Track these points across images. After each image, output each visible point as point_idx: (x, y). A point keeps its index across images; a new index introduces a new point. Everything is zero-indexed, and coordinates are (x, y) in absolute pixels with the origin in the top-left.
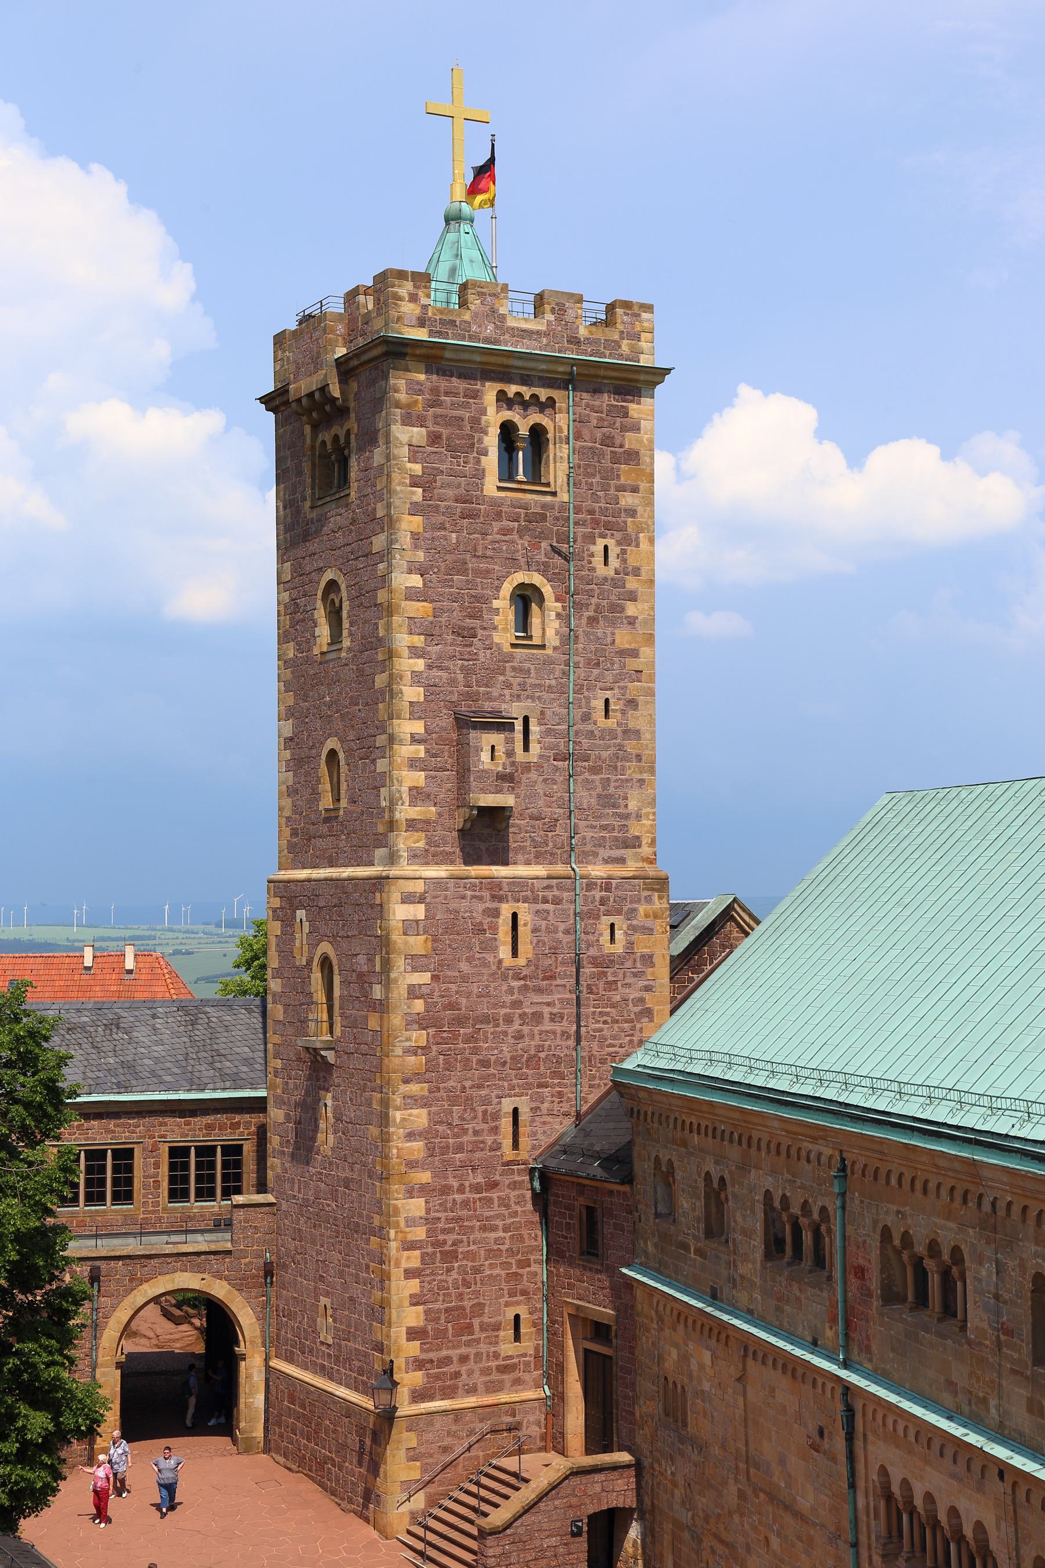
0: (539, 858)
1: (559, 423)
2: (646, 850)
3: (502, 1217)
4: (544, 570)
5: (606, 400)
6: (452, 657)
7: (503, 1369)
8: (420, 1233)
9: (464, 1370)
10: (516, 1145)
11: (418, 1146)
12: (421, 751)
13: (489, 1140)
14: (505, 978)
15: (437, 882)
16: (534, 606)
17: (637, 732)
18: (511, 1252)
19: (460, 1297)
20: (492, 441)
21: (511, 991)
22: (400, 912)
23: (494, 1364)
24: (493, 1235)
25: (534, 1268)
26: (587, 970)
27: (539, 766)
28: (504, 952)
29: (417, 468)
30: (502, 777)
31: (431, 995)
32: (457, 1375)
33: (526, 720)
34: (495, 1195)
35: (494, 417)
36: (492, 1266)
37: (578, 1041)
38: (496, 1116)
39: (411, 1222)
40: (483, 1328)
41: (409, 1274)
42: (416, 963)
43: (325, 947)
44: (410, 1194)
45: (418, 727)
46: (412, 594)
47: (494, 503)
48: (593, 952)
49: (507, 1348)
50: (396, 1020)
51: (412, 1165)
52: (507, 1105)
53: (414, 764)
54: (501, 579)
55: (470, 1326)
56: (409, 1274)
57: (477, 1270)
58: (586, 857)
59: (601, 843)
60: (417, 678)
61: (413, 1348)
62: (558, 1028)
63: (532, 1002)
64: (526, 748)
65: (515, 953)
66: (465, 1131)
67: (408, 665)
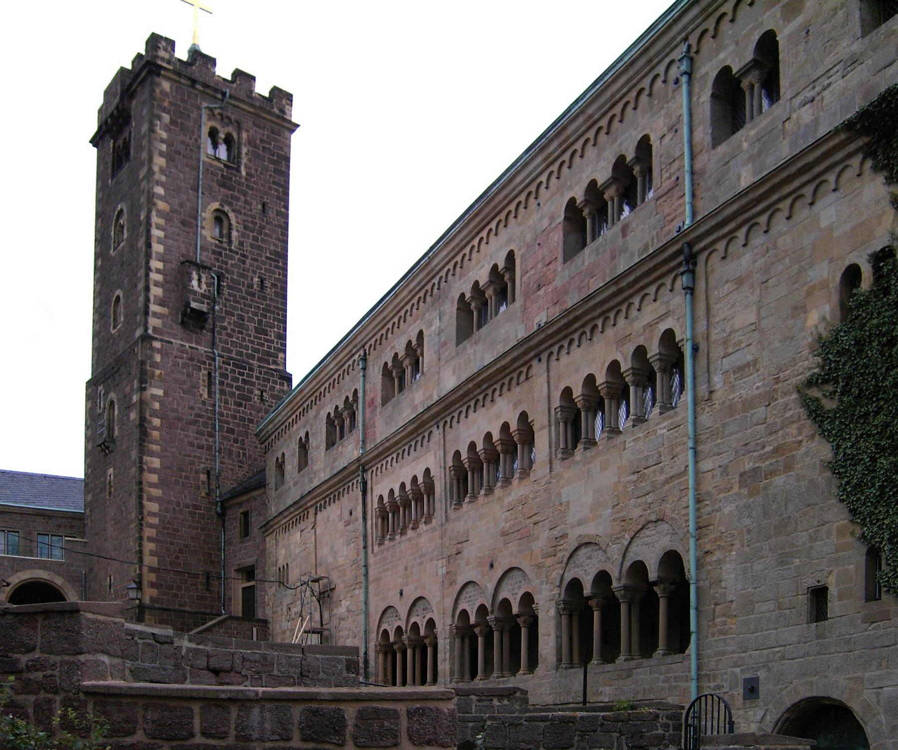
6: (178, 235)
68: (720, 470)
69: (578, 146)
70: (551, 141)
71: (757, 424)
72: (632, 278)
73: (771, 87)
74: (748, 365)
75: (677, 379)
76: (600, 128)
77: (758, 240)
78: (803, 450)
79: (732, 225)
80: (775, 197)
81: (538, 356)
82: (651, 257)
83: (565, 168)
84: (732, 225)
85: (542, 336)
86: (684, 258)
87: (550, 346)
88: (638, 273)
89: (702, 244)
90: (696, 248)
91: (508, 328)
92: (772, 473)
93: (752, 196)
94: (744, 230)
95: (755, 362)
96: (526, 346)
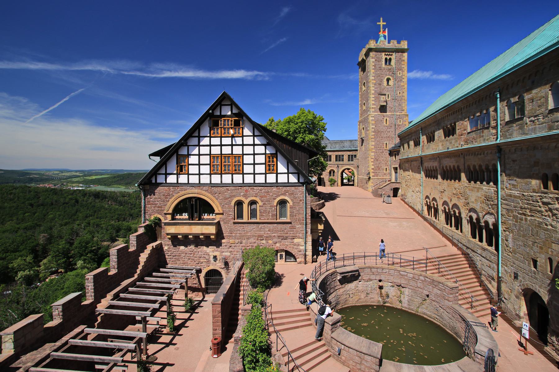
4: (391, 76)
5: (400, 54)
11: (373, 147)
20: (384, 60)
22: (371, 118)
28: (385, 123)
35: (384, 57)
42: (373, 124)
46: (373, 80)
50: (370, 131)
53: (373, 101)
58: (396, 112)
60: (373, 90)
67: (372, 88)
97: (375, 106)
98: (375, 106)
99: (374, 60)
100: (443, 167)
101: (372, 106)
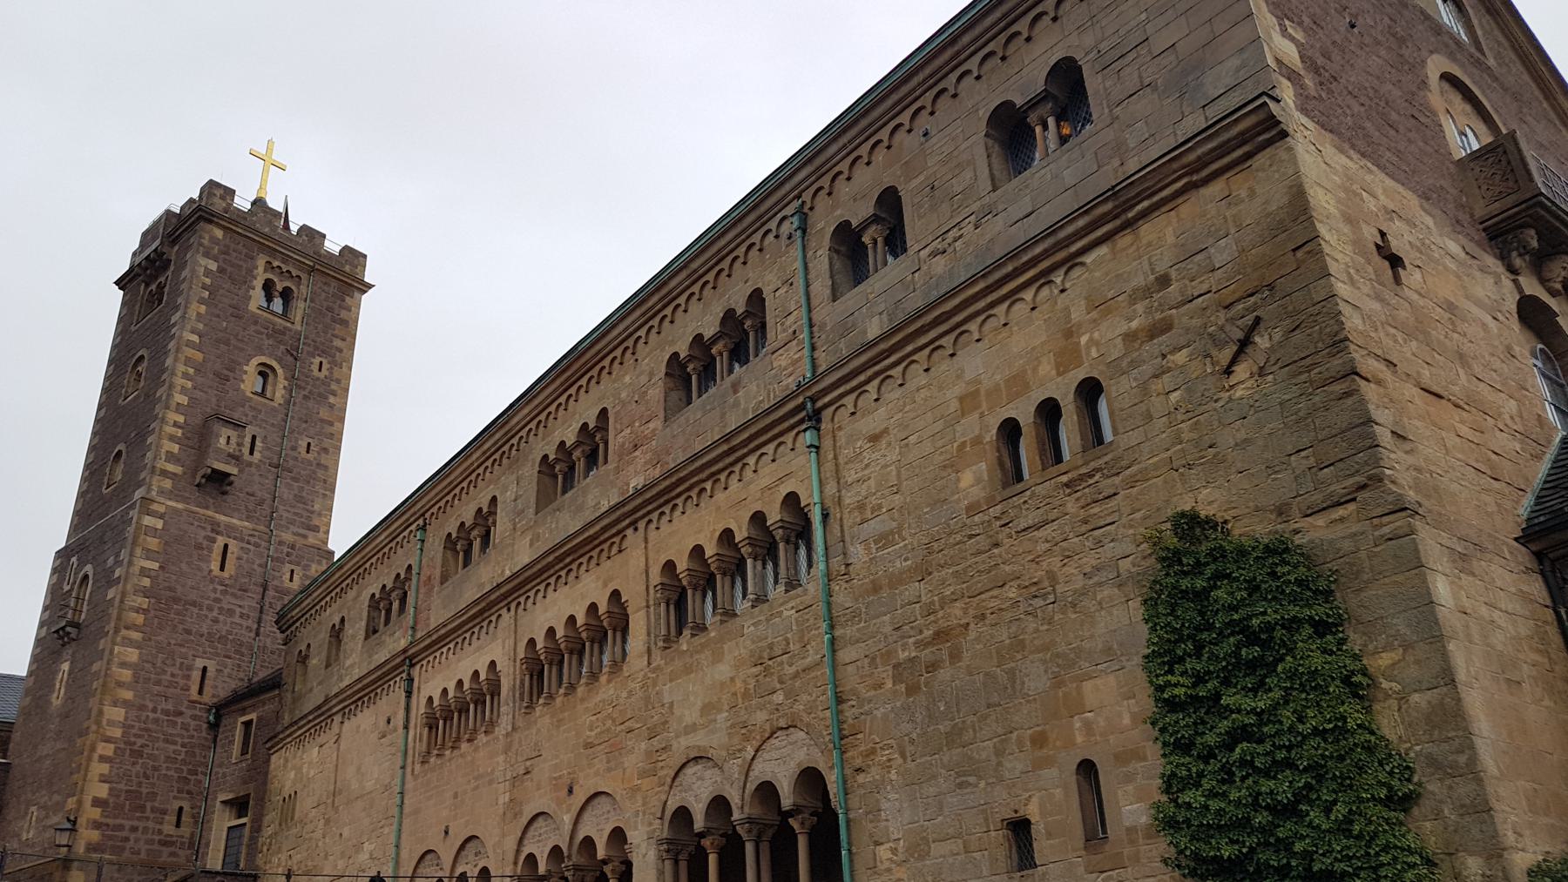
0: (248, 518)
1: (302, 290)
2: (321, 535)
3: (182, 736)
4: (279, 361)
7: (164, 843)
8: (117, 733)
9: (132, 836)
10: (200, 692)
11: (127, 675)
12: (180, 433)
13: (182, 682)
14: (212, 581)
15: (175, 510)
16: (271, 377)
17: (326, 468)
18: (184, 762)
19: (140, 784)
20: (258, 283)
21: (215, 590)
23: (157, 838)
24: (173, 747)
25: (200, 777)
26: (271, 593)
27: (258, 466)
28: (215, 566)
29: (208, 281)
30: (230, 455)
31: (156, 577)
32: (127, 839)
33: (254, 438)
34: (179, 720)
36: (168, 769)
37: (257, 634)
38: (190, 668)
39: (111, 723)
40: (153, 810)
41: (103, 759)
43: (89, 568)
44: (115, 704)
45: (181, 419)
46: (189, 344)
47: (254, 315)
48: (276, 583)
49: (168, 828)
51: (120, 684)
52: (199, 663)
53: (172, 438)
54: (251, 357)
55: (142, 808)
56: (103, 759)
57: (155, 769)
59: (292, 522)
61: (96, 813)
62: (245, 623)
63: (227, 603)
64: (251, 453)
65: (222, 569)
66: (164, 672)
67: (179, 381)
68: (867, 661)
69: (682, 300)
70: (652, 294)
71: (910, 603)
72: (745, 435)
73: (896, 243)
74: (892, 532)
75: (802, 552)
76: (707, 282)
77: (892, 394)
78: (972, 635)
79: (862, 378)
80: (909, 348)
81: (634, 524)
82: (768, 412)
83: (666, 323)
84: (862, 378)
85: (639, 501)
86: (806, 411)
87: (649, 513)
88: (753, 430)
89: (827, 399)
90: (819, 404)
91: (597, 495)
92: (933, 667)
93: (883, 346)
94: (876, 382)
95: (900, 528)
96: (618, 513)
97: (178, 470)
98: (178, 470)
99: (213, 266)
100: (532, 642)
101: (161, 464)
